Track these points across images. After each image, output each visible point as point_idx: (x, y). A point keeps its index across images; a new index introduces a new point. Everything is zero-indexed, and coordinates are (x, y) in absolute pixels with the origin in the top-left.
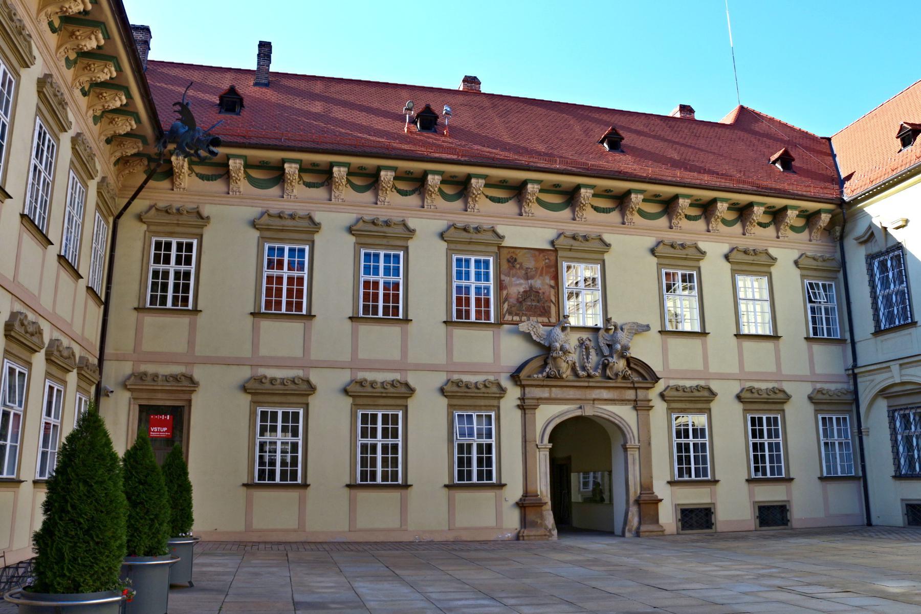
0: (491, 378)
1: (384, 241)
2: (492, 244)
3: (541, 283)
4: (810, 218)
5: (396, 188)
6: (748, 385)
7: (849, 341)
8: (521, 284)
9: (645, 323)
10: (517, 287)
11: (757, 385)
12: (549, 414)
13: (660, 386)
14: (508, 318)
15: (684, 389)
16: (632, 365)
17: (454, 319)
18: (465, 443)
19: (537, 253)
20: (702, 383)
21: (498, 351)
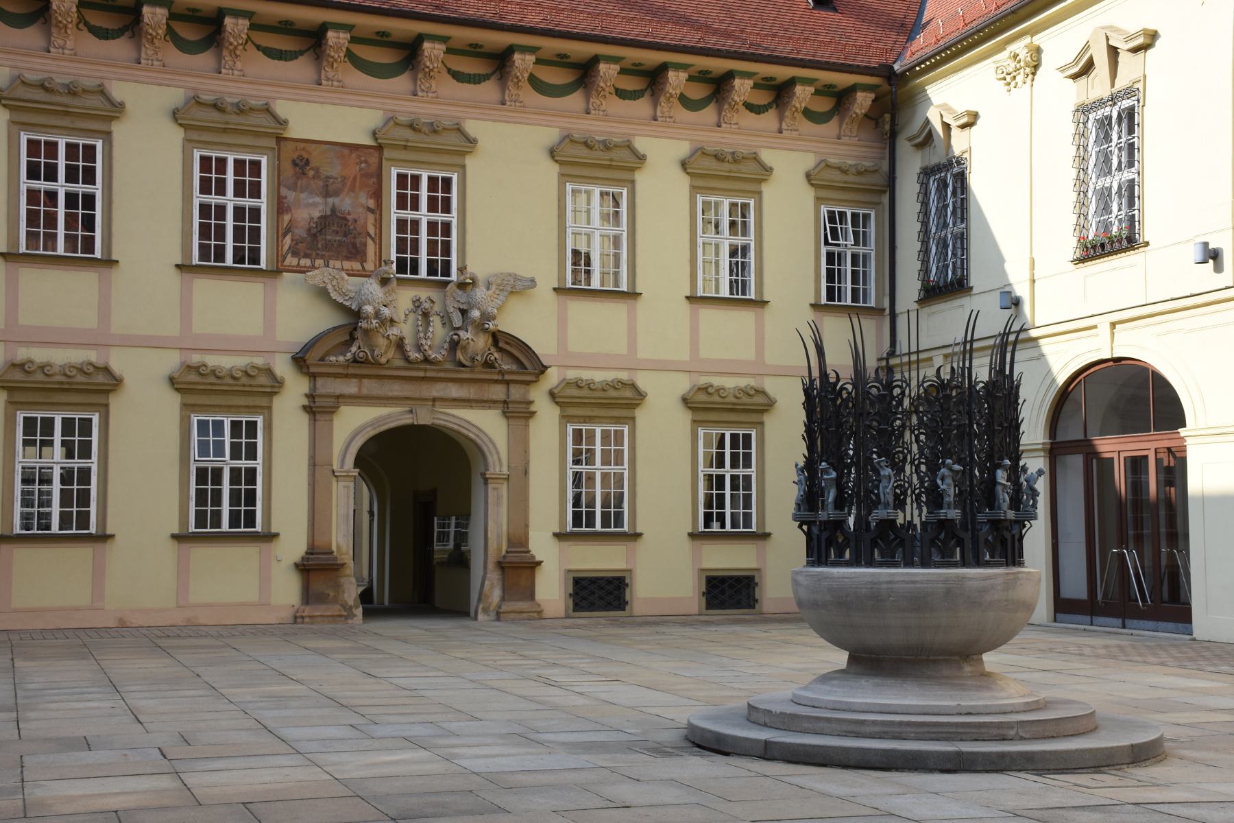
0: (259, 361)
1: (66, 122)
2: (266, 135)
3: (351, 203)
4: (842, 98)
5: (86, 24)
6: (703, 380)
7: (887, 311)
8: (315, 205)
9: (529, 275)
10: (308, 209)
11: (717, 381)
12: (355, 423)
13: (553, 378)
14: (291, 261)
15: (590, 385)
16: (501, 344)
17: (196, 261)
18: (210, 465)
19: (346, 151)
20: (624, 376)
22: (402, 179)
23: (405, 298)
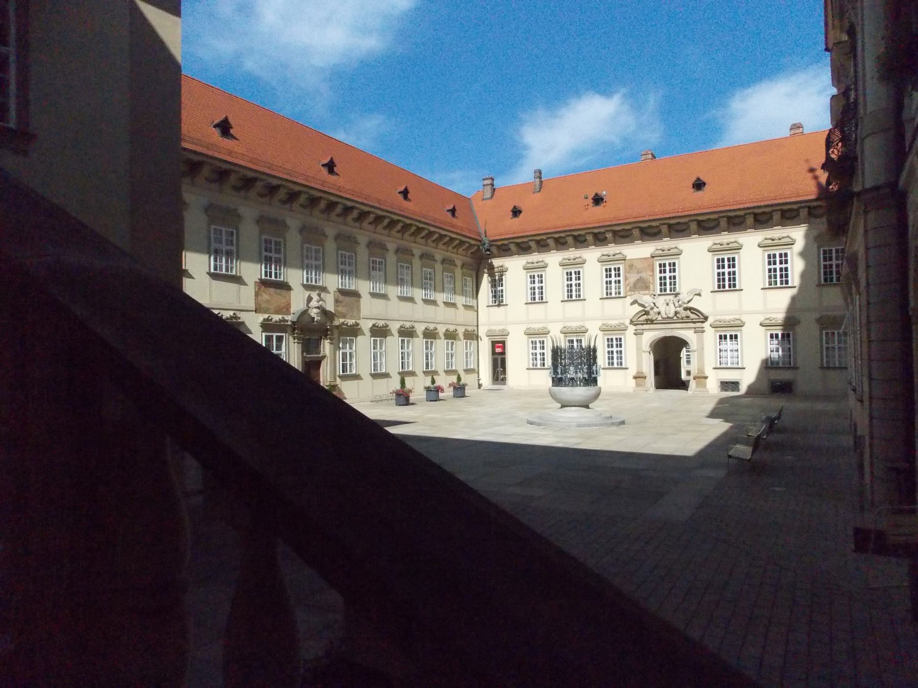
3: (645, 275)
10: (633, 278)
21: (623, 310)
22: (660, 265)
23: (661, 301)
